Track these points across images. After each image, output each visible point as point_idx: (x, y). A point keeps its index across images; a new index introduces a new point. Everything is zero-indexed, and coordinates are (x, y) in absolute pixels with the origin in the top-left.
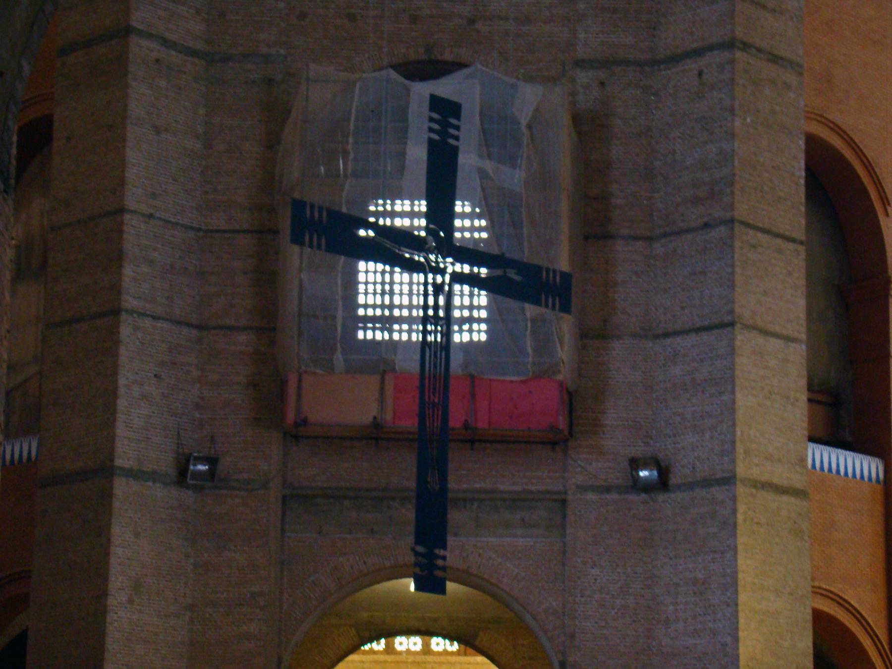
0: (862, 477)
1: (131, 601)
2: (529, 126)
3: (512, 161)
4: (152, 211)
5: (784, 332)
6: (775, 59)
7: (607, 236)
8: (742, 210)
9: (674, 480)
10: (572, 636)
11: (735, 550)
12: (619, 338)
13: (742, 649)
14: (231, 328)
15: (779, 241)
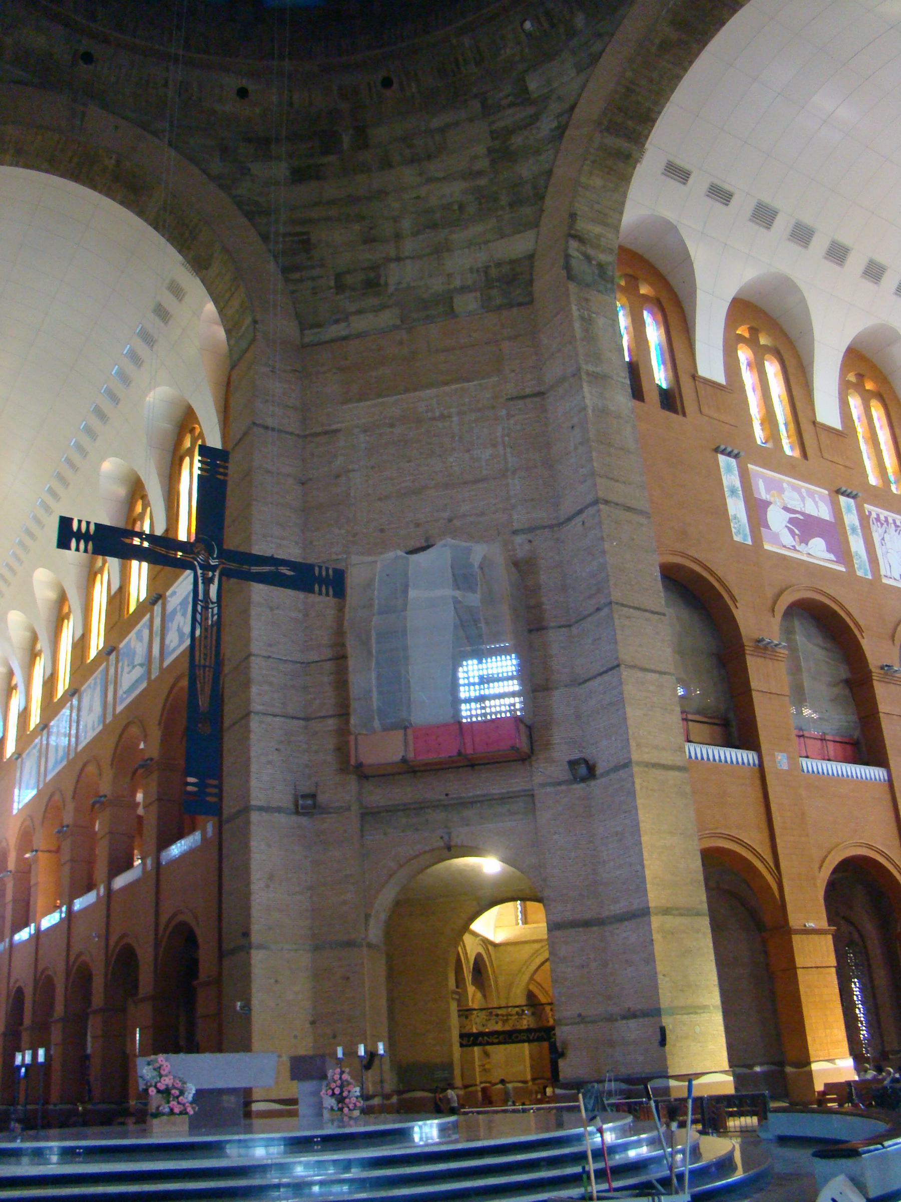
0: (743, 763)
1: (268, 886)
2: (481, 567)
3: (475, 592)
4: (270, 654)
5: (658, 669)
6: (629, 509)
7: (544, 628)
8: (616, 595)
9: (599, 771)
10: (544, 880)
11: (636, 808)
12: (557, 688)
13: (647, 872)
14: (324, 717)
15: (647, 614)
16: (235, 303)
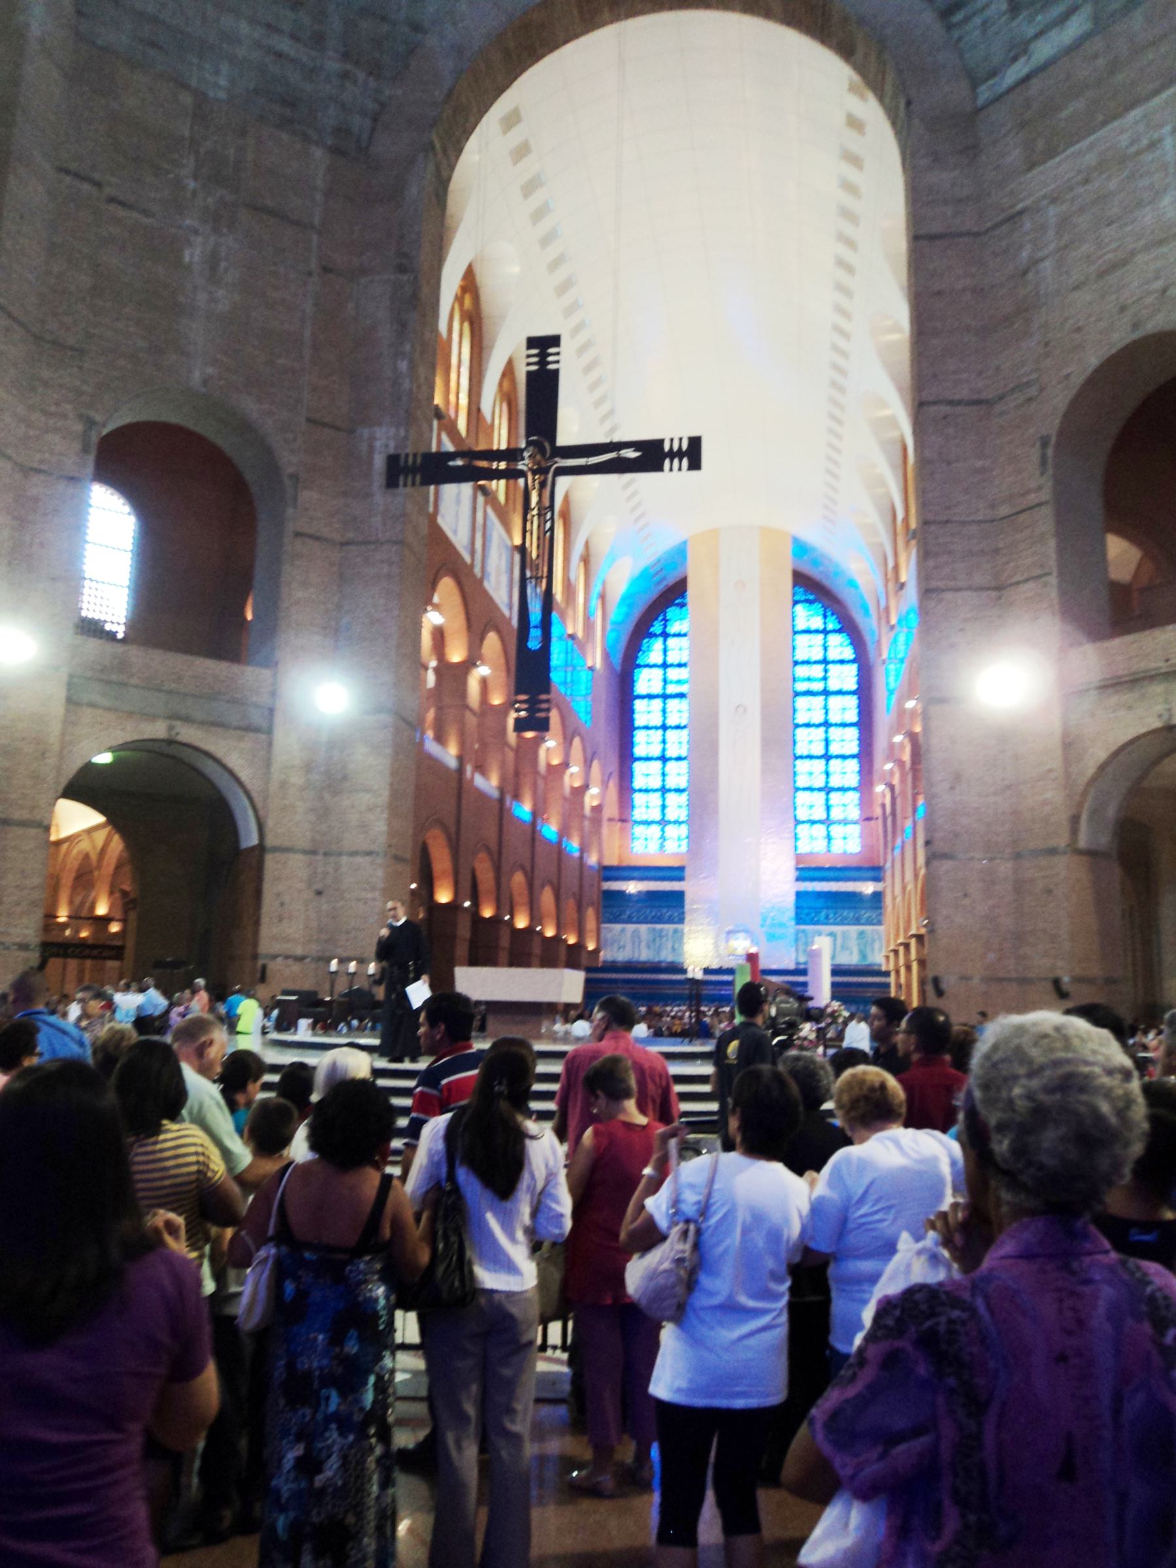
14: (1018, 583)
16: (888, 88)
